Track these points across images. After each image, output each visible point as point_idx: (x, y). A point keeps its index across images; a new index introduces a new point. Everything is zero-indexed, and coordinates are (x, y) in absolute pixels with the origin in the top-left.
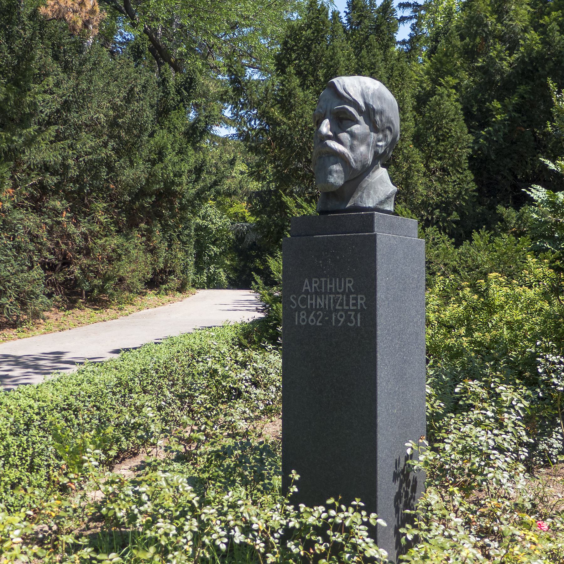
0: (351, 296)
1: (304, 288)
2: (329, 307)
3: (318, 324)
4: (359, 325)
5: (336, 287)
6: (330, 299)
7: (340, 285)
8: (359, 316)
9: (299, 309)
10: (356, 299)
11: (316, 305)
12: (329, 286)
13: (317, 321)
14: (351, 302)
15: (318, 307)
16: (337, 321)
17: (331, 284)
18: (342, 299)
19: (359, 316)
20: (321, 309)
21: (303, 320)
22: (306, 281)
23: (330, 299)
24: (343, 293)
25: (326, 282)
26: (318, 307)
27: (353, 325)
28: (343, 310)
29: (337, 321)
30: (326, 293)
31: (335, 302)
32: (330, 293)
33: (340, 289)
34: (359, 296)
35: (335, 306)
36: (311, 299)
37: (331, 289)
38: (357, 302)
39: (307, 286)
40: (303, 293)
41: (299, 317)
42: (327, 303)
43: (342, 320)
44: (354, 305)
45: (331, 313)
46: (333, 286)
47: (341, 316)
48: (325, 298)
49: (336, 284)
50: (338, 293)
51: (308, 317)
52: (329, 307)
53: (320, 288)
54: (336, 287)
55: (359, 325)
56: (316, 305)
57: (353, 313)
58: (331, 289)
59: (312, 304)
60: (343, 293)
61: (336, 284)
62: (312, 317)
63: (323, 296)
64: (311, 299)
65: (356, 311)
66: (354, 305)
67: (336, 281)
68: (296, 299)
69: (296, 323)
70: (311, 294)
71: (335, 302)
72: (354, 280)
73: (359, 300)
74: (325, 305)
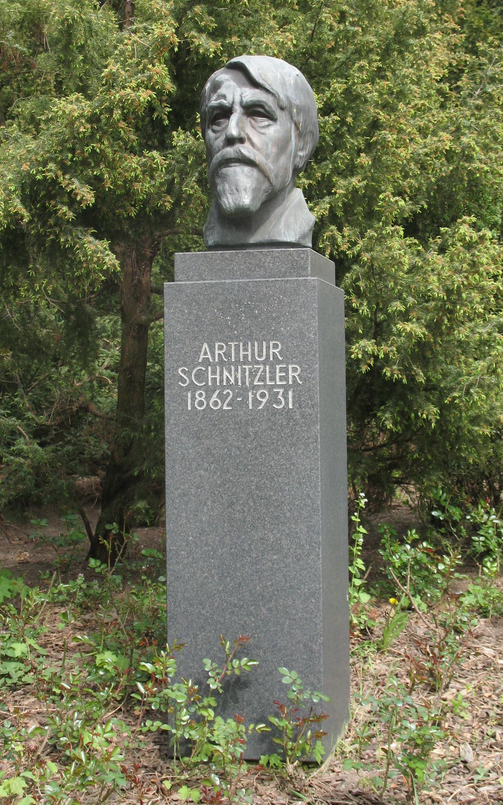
0: (278, 367)
1: (202, 357)
2: (243, 383)
3: (225, 408)
4: (291, 406)
5: (253, 354)
6: (244, 371)
7: (260, 351)
8: (290, 393)
9: (193, 388)
10: (286, 370)
11: (221, 381)
12: (242, 353)
13: (223, 403)
14: (278, 375)
15: (225, 384)
16: (256, 402)
17: (245, 350)
18: (264, 371)
19: (290, 393)
20: (229, 386)
21: (201, 403)
22: (205, 345)
23: (244, 371)
24: (264, 363)
25: (237, 347)
26: (225, 384)
27: (281, 406)
28: (265, 386)
29: (256, 402)
30: (237, 362)
31: (253, 375)
32: (244, 363)
33: (260, 356)
34: (290, 367)
35: (252, 381)
36: (214, 373)
37: (245, 356)
38: (287, 374)
39: (206, 353)
40: (199, 364)
41: (193, 398)
42: (239, 376)
43: (264, 400)
44: (281, 378)
45: (246, 390)
46: (249, 353)
47: (263, 395)
48: (236, 370)
49: (253, 350)
50: (258, 363)
51: (208, 398)
52: (243, 383)
53: (228, 355)
54: (253, 354)
55: (291, 406)
56: (221, 381)
57: (281, 391)
58: (245, 356)
59: (214, 380)
60: (264, 363)
61: (253, 350)
62: (214, 398)
63: (233, 368)
64: (214, 373)
65: (286, 388)
66: (281, 378)
67: (253, 345)
68: (189, 374)
69: (189, 408)
70: (214, 366)
71: (253, 375)
72: (282, 344)
73: (290, 372)
74: (236, 380)
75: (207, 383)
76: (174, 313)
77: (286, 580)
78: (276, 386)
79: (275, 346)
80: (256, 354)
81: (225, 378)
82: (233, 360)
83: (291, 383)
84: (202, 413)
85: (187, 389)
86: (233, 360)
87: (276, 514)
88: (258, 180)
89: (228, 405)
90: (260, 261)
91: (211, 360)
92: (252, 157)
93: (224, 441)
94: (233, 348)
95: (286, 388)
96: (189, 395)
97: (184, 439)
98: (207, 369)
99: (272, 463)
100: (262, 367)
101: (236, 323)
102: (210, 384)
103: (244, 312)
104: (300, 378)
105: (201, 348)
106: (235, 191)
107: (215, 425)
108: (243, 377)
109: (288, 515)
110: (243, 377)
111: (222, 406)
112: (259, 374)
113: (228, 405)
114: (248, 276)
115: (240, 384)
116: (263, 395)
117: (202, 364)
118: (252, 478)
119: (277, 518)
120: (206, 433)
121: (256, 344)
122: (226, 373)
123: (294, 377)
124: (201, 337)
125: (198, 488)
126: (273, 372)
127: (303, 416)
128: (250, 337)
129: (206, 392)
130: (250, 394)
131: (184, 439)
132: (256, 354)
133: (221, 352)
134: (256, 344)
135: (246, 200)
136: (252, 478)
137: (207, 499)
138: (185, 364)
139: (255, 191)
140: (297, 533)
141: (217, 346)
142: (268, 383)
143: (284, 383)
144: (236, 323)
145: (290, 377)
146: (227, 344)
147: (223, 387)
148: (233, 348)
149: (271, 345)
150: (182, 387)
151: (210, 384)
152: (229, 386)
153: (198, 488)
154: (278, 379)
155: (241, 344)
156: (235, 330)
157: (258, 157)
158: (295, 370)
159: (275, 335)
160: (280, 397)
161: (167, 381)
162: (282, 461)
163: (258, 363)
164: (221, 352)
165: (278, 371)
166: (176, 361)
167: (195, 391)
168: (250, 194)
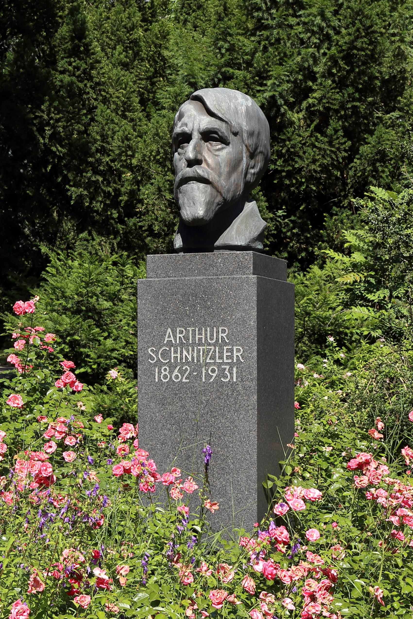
1: (166, 339)
2: (198, 361)
3: (184, 380)
4: (235, 380)
5: (206, 337)
6: (199, 351)
7: (212, 335)
8: (235, 369)
9: (159, 364)
10: (232, 351)
11: (181, 359)
12: (197, 336)
16: (208, 376)
17: (200, 334)
19: (235, 369)
20: (187, 363)
21: (165, 377)
22: (169, 330)
23: (199, 351)
25: (194, 331)
27: (228, 380)
28: (214, 363)
29: (208, 376)
30: (194, 344)
32: (199, 345)
33: (211, 339)
34: (235, 348)
36: (176, 352)
37: (200, 339)
38: (232, 353)
39: (169, 337)
40: (164, 345)
41: (160, 373)
43: (214, 375)
45: (201, 366)
46: (203, 337)
47: (213, 371)
48: (193, 350)
49: (206, 334)
50: (209, 344)
51: (171, 372)
52: (198, 361)
53: (186, 338)
54: (206, 337)
55: (235, 380)
56: (181, 359)
57: (228, 367)
58: (200, 339)
61: (206, 334)
62: (176, 372)
64: (176, 352)
65: (231, 365)
67: (206, 330)
68: (156, 353)
69: (157, 381)
70: (176, 347)
73: (235, 352)
75: (170, 361)
76: (145, 304)
77: (229, 518)
78: (223, 363)
79: (223, 331)
80: (208, 338)
81: (184, 356)
82: (191, 342)
83: (235, 361)
84: (166, 385)
85: (155, 365)
86: (191, 342)
87: (223, 466)
88: (211, 194)
89: (186, 378)
90: (213, 261)
91: (173, 342)
92: (206, 176)
93: (183, 407)
94: (191, 332)
95: (231, 365)
96: (157, 370)
97: (153, 405)
98: (170, 349)
99: (220, 425)
100: (212, 348)
101: (193, 312)
102: (172, 361)
103: (200, 304)
104: (242, 358)
105: (166, 332)
106: (192, 204)
107: (176, 394)
108: (198, 356)
109: (232, 466)
110: (198, 356)
111: (182, 379)
112: (210, 353)
113: (186, 378)
114: (204, 274)
115: (195, 361)
116: (213, 371)
117: (166, 345)
118: (204, 437)
119: (223, 469)
120: (169, 400)
121: (208, 329)
122: (185, 353)
123: (237, 356)
124: (166, 324)
125: (162, 444)
126: (221, 353)
127: (244, 388)
128: (205, 324)
129: (169, 367)
130: (203, 369)
131: (153, 405)
132: (208, 338)
133: (181, 336)
134: (208, 329)
135: (200, 212)
136: (204, 437)
137: (170, 453)
138: (153, 345)
139: (209, 204)
140: (238, 481)
141: (178, 331)
142: (218, 361)
143: (230, 361)
144: (193, 312)
145: (235, 356)
146: (186, 329)
147: (183, 364)
148: (191, 332)
149: (220, 330)
150: (151, 364)
151: (172, 361)
152: (187, 363)
153: (162, 444)
154: (225, 358)
155: (197, 329)
156: (192, 318)
157: (212, 176)
158: (238, 351)
159: (223, 322)
160: (226, 372)
161: (140, 359)
162: (228, 424)
163: (209, 344)
164: (181, 336)
165: (225, 351)
166: (147, 342)
167: (161, 367)
168: (204, 206)
